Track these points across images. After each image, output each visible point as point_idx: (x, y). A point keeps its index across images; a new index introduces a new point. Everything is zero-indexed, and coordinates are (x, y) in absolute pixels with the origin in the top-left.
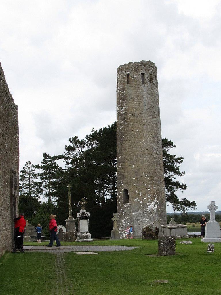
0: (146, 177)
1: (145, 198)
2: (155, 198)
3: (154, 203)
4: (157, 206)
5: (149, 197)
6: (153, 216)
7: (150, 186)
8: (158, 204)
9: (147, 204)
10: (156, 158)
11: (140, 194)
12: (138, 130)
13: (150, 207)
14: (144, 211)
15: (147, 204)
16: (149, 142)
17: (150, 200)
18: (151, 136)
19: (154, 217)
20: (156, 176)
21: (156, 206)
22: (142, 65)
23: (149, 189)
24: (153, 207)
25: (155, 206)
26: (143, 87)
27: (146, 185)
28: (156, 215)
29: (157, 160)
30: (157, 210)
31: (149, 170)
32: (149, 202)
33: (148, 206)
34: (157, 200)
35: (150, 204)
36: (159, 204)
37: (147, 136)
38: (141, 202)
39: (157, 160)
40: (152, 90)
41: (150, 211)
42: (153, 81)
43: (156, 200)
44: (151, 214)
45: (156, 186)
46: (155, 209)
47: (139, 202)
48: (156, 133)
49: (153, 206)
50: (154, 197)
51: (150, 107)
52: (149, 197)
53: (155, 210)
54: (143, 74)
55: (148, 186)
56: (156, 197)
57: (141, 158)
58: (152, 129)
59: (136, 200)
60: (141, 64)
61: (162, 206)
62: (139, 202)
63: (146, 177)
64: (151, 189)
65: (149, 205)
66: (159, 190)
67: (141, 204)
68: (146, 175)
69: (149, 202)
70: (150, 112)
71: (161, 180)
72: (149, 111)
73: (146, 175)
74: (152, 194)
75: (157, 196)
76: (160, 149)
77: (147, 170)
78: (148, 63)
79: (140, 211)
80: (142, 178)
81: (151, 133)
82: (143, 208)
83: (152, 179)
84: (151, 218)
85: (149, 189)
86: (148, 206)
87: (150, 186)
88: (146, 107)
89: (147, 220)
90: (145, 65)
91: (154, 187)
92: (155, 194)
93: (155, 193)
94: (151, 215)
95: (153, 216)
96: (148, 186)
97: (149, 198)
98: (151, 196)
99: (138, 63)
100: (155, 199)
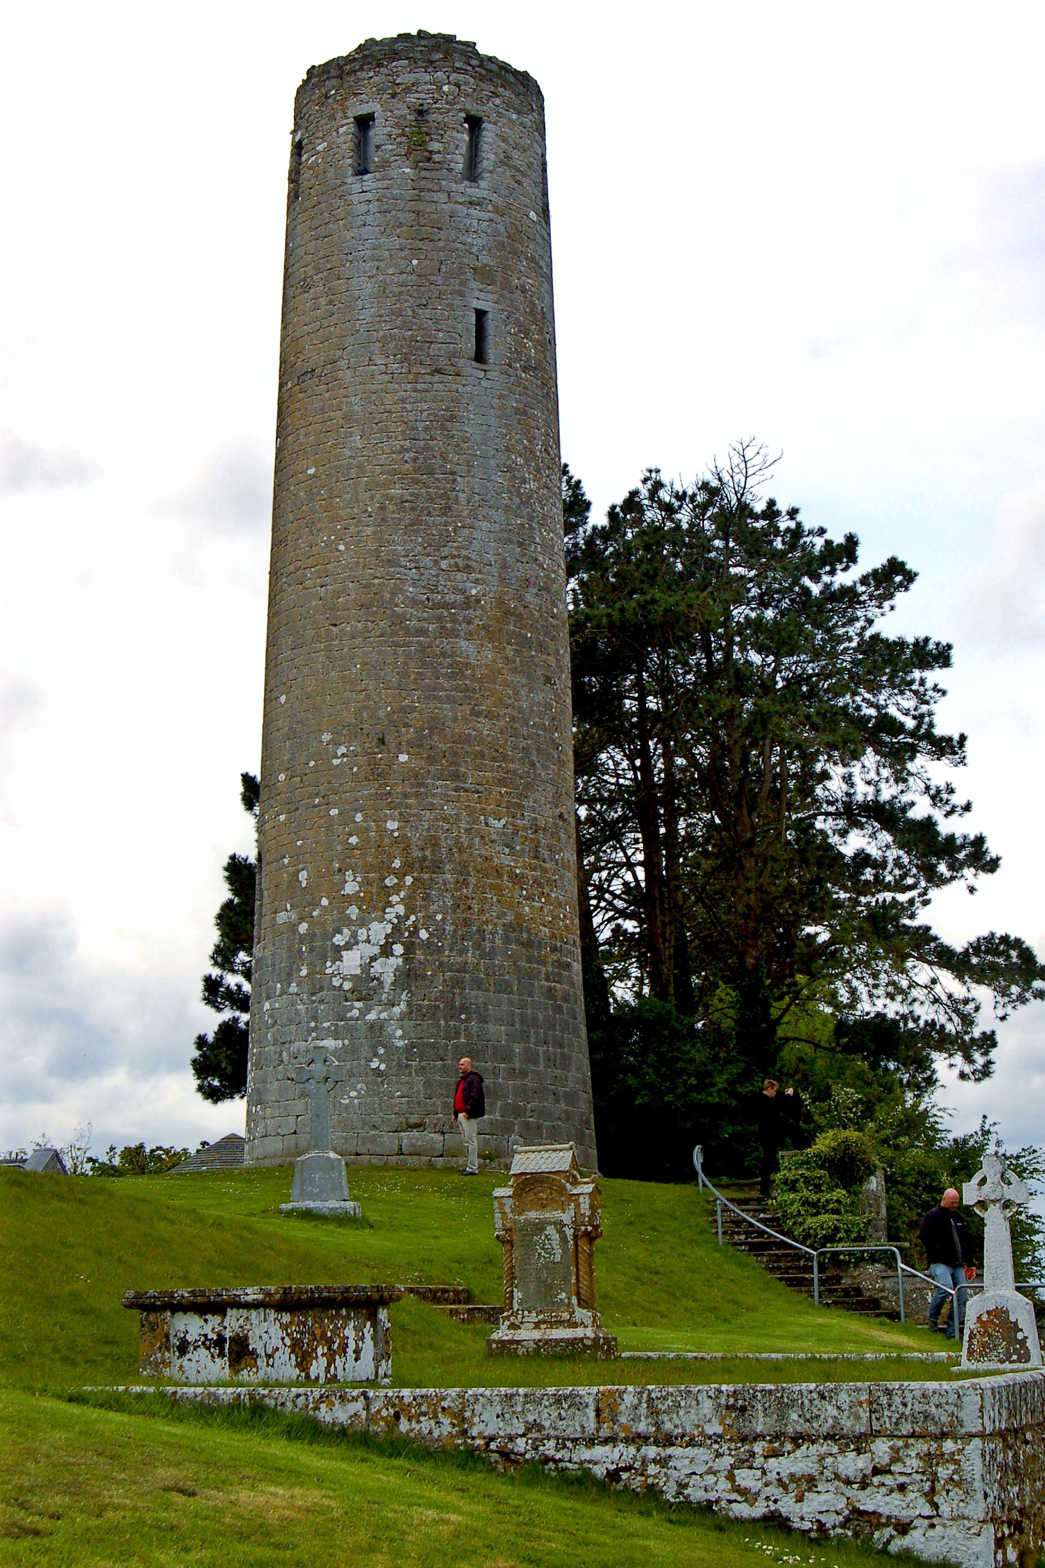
0: (336, 762)
1: (325, 902)
2: (394, 898)
3: (379, 931)
4: (409, 948)
5: (351, 888)
6: (372, 1016)
7: (359, 817)
8: (415, 933)
9: (339, 940)
10: (422, 632)
11: (303, 876)
12: (311, 471)
13: (351, 962)
14: (317, 985)
15: (339, 940)
16: (369, 530)
17: (353, 912)
18: (386, 497)
19: (377, 1029)
20: (415, 746)
21: (398, 949)
22: (361, 69)
23: (354, 840)
24: (373, 959)
25: (386, 951)
26: (355, 198)
27: (334, 812)
28: (397, 1010)
29: (423, 648)
30: (407, 977)
31: (357, 714)
32: (348, 921)
33: (337, 952)
34: (410, 910)
35: (354, 935)
36: (423, 934)
37: (364, 496)
38: (303, 928)
39: (423, 648)
40: (421, 206)
41: (347, 986)
42: (435, 146)
43: (401, 909)
44: (359, 1004)
45: (403, 819)
46: (387, 969)
47: (293, 927)
48: (431, 473)
49: (376, 950)
50: (387, 891)
51: (392, 313)
52: (351, 888)
53: (389, 979)
54: (364, 123)
55: (345, 818)
56: (397, 888)
57: (318, 638)
58: (403, 450)
59: (282, 917)
60: (354, 60)
61: (463, 951)
62: (293, 927)
63: (336, 762)
64: (365, 841)
65: (348, 947)
66: (433, 843)
67: (302, 939)
68: (342, 750)
69: (348, 921)
70: (391, 345)
71: (457, 776)
72: (384, 341)
73: (342, 750)
74: (368, 869)
75: (409, 880)
76: (468, 569)
77: (348, 715)
78: (399, 46)
79: (293, 988)
80: (316, 770)
81: (393, 473)
82: (311, 965)
83: (378, 773)
84: (351, 1031)
85: (354, 840)
86: (338, 949)
87: (359, 817)
88: (367, 315)
89: (330, 1043)
90: (378, 65)
91: (392, 825)
92: (395, 873)
93: (397, 864)
94: (355, 1013)
95: (372, 1016)
96: (345, 818)
97: (350, 900)
98: (366, 883)
99: (349, 59)
100: (390, 905)
